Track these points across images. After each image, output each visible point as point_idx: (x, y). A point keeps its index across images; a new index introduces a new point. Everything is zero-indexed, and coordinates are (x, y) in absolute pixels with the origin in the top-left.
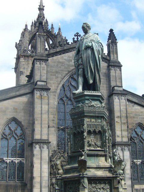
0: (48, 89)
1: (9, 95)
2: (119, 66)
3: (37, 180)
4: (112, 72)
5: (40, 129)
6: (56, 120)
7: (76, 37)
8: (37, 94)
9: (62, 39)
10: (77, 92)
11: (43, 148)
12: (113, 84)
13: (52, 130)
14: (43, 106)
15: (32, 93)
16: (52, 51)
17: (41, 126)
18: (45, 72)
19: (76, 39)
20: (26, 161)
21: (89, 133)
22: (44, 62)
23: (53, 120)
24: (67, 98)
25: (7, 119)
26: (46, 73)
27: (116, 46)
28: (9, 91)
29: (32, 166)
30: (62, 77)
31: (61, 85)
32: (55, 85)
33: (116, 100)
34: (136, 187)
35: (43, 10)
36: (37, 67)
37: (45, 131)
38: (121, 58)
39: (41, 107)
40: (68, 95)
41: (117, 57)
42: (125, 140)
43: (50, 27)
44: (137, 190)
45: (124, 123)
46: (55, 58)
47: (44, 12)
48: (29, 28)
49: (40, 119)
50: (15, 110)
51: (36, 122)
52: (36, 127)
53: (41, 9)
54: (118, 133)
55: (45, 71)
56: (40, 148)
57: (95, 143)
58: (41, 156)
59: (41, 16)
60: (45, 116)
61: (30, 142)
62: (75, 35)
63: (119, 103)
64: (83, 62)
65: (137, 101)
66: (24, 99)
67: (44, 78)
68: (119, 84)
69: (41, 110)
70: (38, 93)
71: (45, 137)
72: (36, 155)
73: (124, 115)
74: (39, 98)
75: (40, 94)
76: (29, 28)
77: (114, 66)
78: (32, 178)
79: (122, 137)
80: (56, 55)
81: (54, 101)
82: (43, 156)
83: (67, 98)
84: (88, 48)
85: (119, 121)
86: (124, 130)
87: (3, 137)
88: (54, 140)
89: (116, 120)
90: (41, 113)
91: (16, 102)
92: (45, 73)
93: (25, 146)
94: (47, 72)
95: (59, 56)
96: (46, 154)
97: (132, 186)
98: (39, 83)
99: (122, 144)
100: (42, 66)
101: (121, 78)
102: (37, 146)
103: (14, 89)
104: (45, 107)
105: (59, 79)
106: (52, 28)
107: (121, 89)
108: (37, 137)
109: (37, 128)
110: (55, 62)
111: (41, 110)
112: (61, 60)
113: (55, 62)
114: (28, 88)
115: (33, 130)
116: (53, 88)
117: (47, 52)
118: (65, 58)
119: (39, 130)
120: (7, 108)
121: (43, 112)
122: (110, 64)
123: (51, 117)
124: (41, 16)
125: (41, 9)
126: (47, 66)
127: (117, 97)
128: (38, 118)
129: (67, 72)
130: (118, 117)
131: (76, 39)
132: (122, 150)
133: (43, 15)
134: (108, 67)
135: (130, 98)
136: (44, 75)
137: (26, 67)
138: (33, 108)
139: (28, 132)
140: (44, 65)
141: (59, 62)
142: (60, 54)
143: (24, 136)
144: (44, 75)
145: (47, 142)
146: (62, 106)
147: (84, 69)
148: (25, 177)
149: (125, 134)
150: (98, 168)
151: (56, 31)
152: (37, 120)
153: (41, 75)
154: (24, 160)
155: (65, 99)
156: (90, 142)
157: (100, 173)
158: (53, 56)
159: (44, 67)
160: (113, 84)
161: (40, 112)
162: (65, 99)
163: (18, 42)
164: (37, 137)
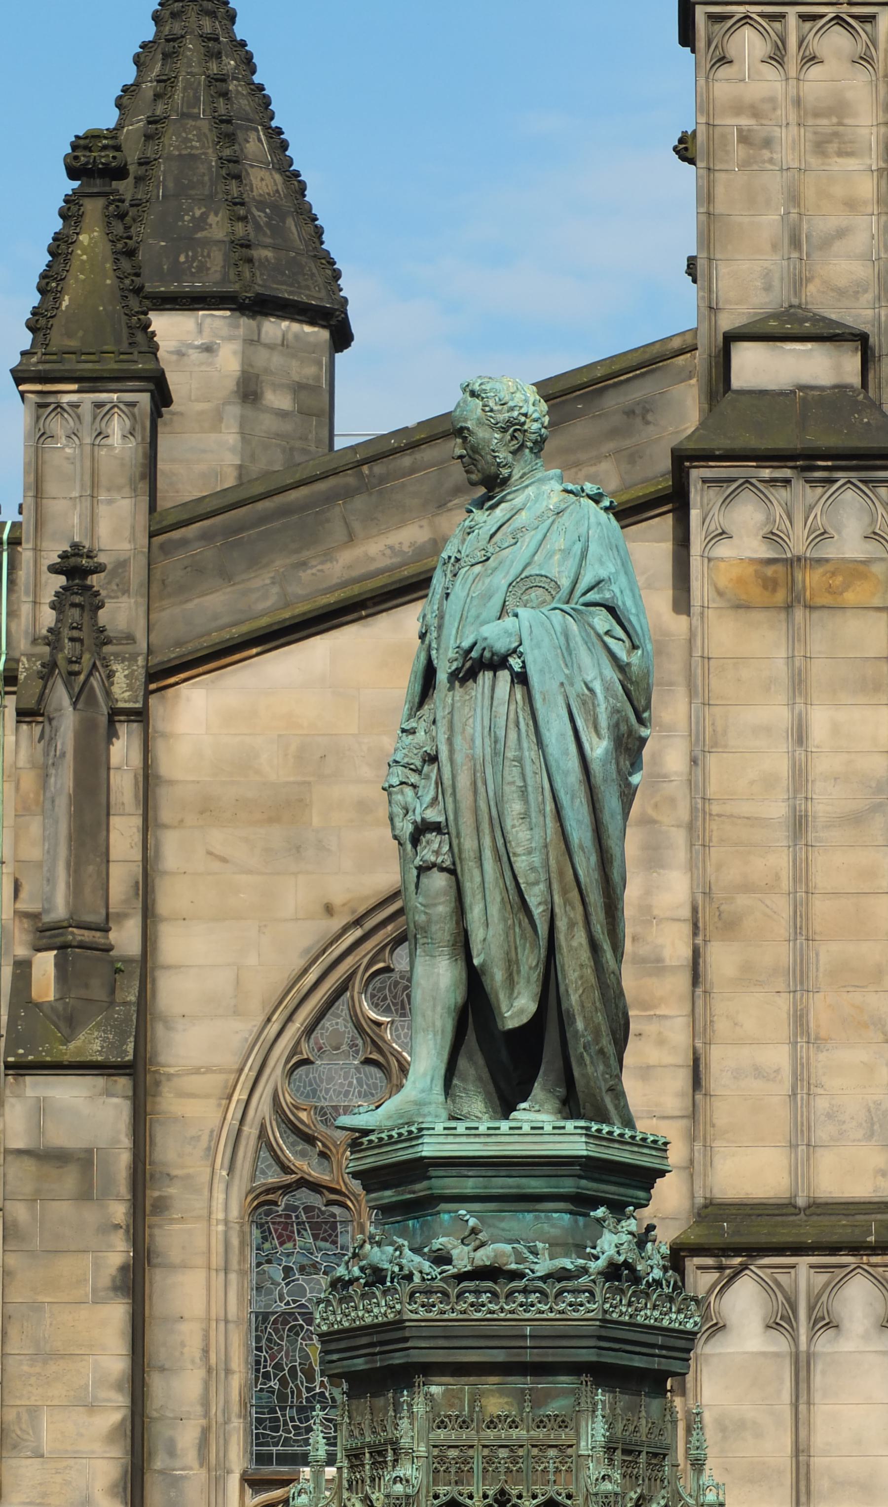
1: (346, 557)
5: (778, 1057)
11: (825, 1322)
14: (820, 719)
17: (799, 1020)
22: (838, 20)
25: (329, 910)
26: (867, 189)
28: (330, 498)
36: (738, 108)
39: (800, 734)
49: (782, 906)
51: (722, 960)
52: (721, 1026)
55: (852, 164)
56: (781, 1321)
58: (800, 1452)
69: (800, 777)
72: (734, 1428)
74: (756, 593)
75: (771, 537)
82: (821, 1437)
87: (286, 1169)
90: (799, 824)
92: (851, 204)
100: (817, 82)
102: (744, 1303)
103: (406, 461)
111: (800, 777)
114: (614, 433)
119: (758, 1072)
120: (316, 760)
121: (826, 801)
128: (742, 901)
136: (841, 233)
144: (841, 233)
152: (730, 926)
159: (838, 109)
161: (777, 809)
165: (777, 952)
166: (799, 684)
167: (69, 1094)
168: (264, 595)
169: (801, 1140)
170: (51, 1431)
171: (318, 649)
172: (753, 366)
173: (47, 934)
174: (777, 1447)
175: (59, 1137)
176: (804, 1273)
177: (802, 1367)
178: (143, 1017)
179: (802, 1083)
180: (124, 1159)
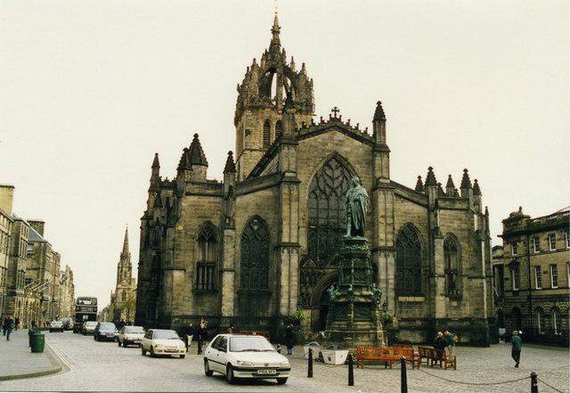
0: (299, 182)
2: (385, 151)
3: (285, 289)
4: (378, 160)
6: (307, 218)
7: (333, 114)
8: (285, 190)
9: (307, 81)
10: (346, 236)
12: (378, 174)
13: (302, 230)
15: (278, 185)
16: (303, 133)
18: (294, 159)
19: (333, 116)
21: (355, 269)
24: (320, 190)
27: (385, 124)
31: (313, 175)
32: (306, 177)
33: (381, 196)
34: (401, 299)
35: (278, 32)
37: (294, 233)
38: (391, 141)
40: (322, 187)
41: (385, 139)
42: (390, 244)
43: (288, 61)
44: (401, 302)
46: (307, 140)
47: (280, 36)
48: (259, 62)
53: (275, 31)
54: (382, 236)
56: (289, 252)
59: (275, 44)
60: (294, 216)
61: (276, 245)
62: (332, 111)
63: (385, 201)
65: (407, 196)
66: (268, 193)
67: (293, 167)
68: (385, 174)
70: (286, 186)
71: (294, 240)
73: (389, 214)
76: (259, 62)
77: (381, 152)
78: (279, 287)
79: (387, 241)
81: (304, 194)
83: (320, 190)
84: (356, 201)
85: (383, 222)
86: (389, 233)
88: (303, 243)
89: (381, 220)
91: (260, 196)
94: (297, 159)
95: (312, 138)
96: (295, 260)
97: (396, 299)
98: (287, 174)
99: (386, 249)
101: (388, 167)
102: (285, 251)
105: (311, 168)
106: (292, 63)
107: (388, 181)
108: (285, 239)
110: (306, 146)
112: (314, 144)
113: (306, 146)
115: (280, 232)
116: (302, 178)
117: (296, 134)
120: (248, 204)
122: (376, 149)
123: (302, 214)
124: (275, 44)
125: (275, 31)
126: (298, 151)
127: (381, 192)
130: (382, 216)
131: (333, 116)
132: (385, 256)
133: (279, 41)
134: (373, 151)
135: (399, 191)
137: (254, 122)
138: (280, 205)
139: (273, 233)
140: (293, 150)
141: (311, 146)
142: (313, 136)
145: (297, 246)
146: (314, 201)
149: (390, 237)
150: (362, 296)
151: (298, 69)
153: (289, 164)
155: (318, 192)
157: (362, 300)
160: (378, 174)
162: (318, 192)
163: (241, 84)
164: (285, 239)
165: (288, 222)
167: (230, 231)
168: (244, 190)
171: (248, 196)
178: (234, 225)
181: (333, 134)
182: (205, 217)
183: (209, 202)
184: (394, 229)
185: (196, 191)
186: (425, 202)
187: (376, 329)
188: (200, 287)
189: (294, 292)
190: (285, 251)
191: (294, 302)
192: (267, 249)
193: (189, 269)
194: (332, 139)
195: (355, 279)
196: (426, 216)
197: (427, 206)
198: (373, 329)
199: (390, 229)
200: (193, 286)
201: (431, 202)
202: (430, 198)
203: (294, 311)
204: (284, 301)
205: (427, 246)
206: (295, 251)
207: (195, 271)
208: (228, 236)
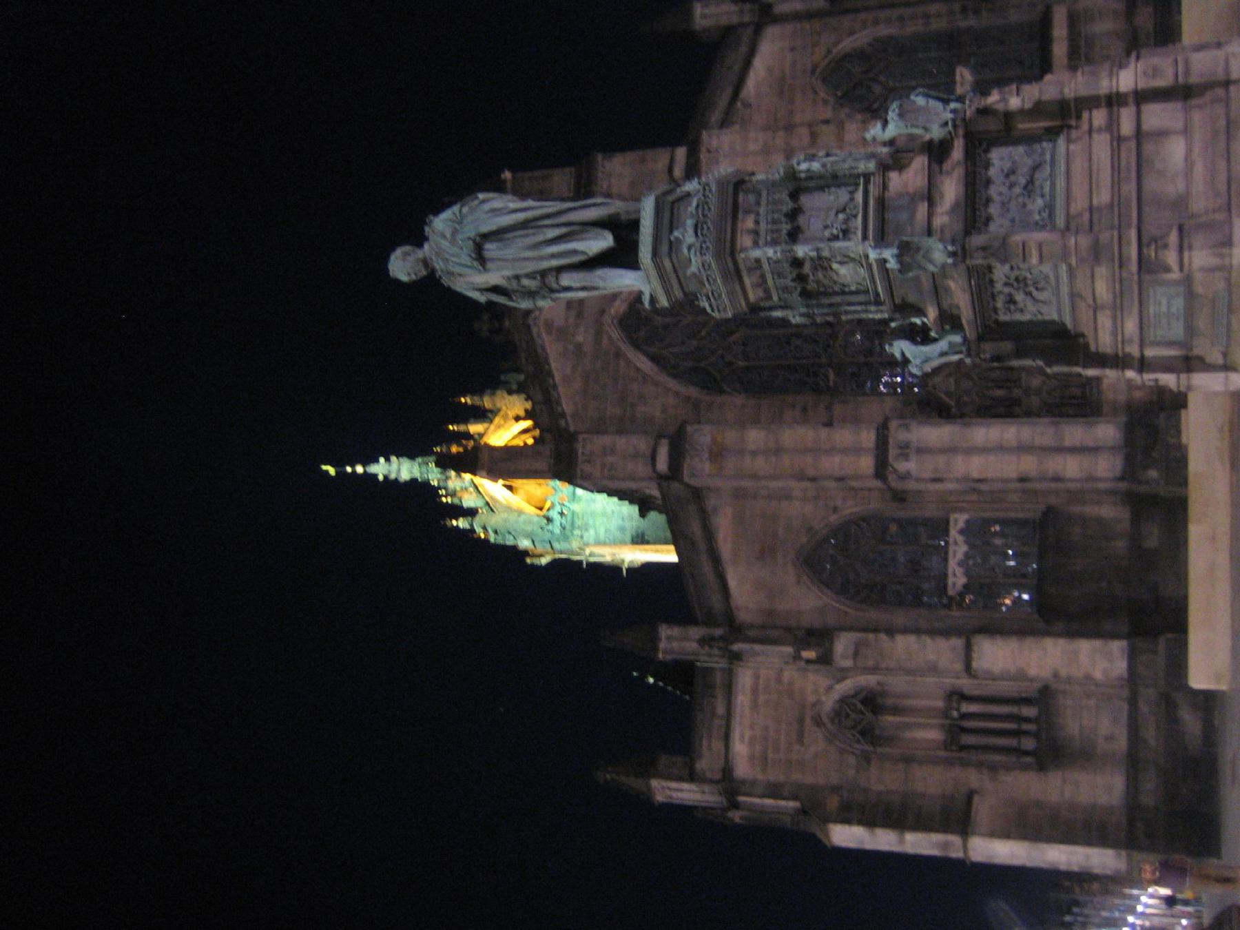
3: (1029, 465)
5: (837, 459)
18: (621, 442)
20: (961, 510)
21: (794, 236)
23: (804, 409)
26: (624, 440)
29: (975, 486)
30: (640, 379)
37: (843, 436)
39: (754, 453)
45: (814, 136)
46: (567, 406)
50: (766, 552)
51: (811, 472)
56: (906, 457)
57: (837, 213)
64: (535, 272)
65: (729, 91)
71: (868, 437)
80: (559, 403)
93: (902, 514)
104: (755, 437)
108: (866, 464)
109: (833, 464)
118: (568, 371)
129: (622, 363)
142: (555, 386)
143: (864, 520)
147: (560, 270)
148: (1021, 515)
154: (956, 521)
156: (835, 231)
157: (951, 189)
158: (563, 415)
166: (741, 452)
169: (857, 451)
170: (932, 657)
171: (732, 583)
172: (662, 465)
173: (797, 652)
174: (941, 460)
175: (851, 651)
176: (892, 452)
177: (921, 451)
179: (844, 451)
180: (859, 635)
181: (549, 326)
182: (801, 721)
183: (755, 706)
184: (826, 122)
185: (718, 745)
186: (749, 31)
187: (1114, 101)
188: (1028, 744)
189: (1038, 432)
190: (903, 466)
191: (1074, 433)
192: (901, 523)
193: (973, 778)
194: (562, 334)
195: (846, 233)
196: (789, 28)
197: (758, 30)
198: (1112, 125)
199: (827, 132)
200: (1025, 768)
201: (747, 18)
202: (735, 20)
203: (1107, 432)
204: (1072, 467)
205: (883, 14)
206: (903, 436)
207: (975, 757)
208: (856, 654)
